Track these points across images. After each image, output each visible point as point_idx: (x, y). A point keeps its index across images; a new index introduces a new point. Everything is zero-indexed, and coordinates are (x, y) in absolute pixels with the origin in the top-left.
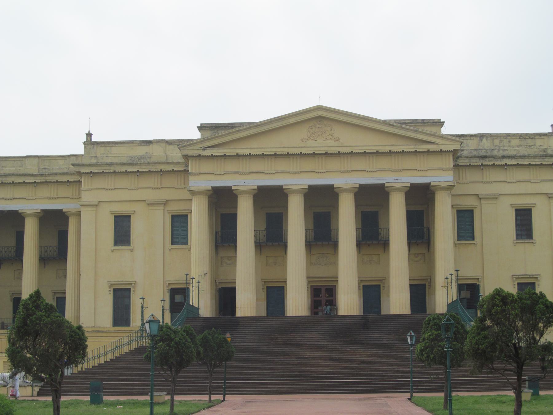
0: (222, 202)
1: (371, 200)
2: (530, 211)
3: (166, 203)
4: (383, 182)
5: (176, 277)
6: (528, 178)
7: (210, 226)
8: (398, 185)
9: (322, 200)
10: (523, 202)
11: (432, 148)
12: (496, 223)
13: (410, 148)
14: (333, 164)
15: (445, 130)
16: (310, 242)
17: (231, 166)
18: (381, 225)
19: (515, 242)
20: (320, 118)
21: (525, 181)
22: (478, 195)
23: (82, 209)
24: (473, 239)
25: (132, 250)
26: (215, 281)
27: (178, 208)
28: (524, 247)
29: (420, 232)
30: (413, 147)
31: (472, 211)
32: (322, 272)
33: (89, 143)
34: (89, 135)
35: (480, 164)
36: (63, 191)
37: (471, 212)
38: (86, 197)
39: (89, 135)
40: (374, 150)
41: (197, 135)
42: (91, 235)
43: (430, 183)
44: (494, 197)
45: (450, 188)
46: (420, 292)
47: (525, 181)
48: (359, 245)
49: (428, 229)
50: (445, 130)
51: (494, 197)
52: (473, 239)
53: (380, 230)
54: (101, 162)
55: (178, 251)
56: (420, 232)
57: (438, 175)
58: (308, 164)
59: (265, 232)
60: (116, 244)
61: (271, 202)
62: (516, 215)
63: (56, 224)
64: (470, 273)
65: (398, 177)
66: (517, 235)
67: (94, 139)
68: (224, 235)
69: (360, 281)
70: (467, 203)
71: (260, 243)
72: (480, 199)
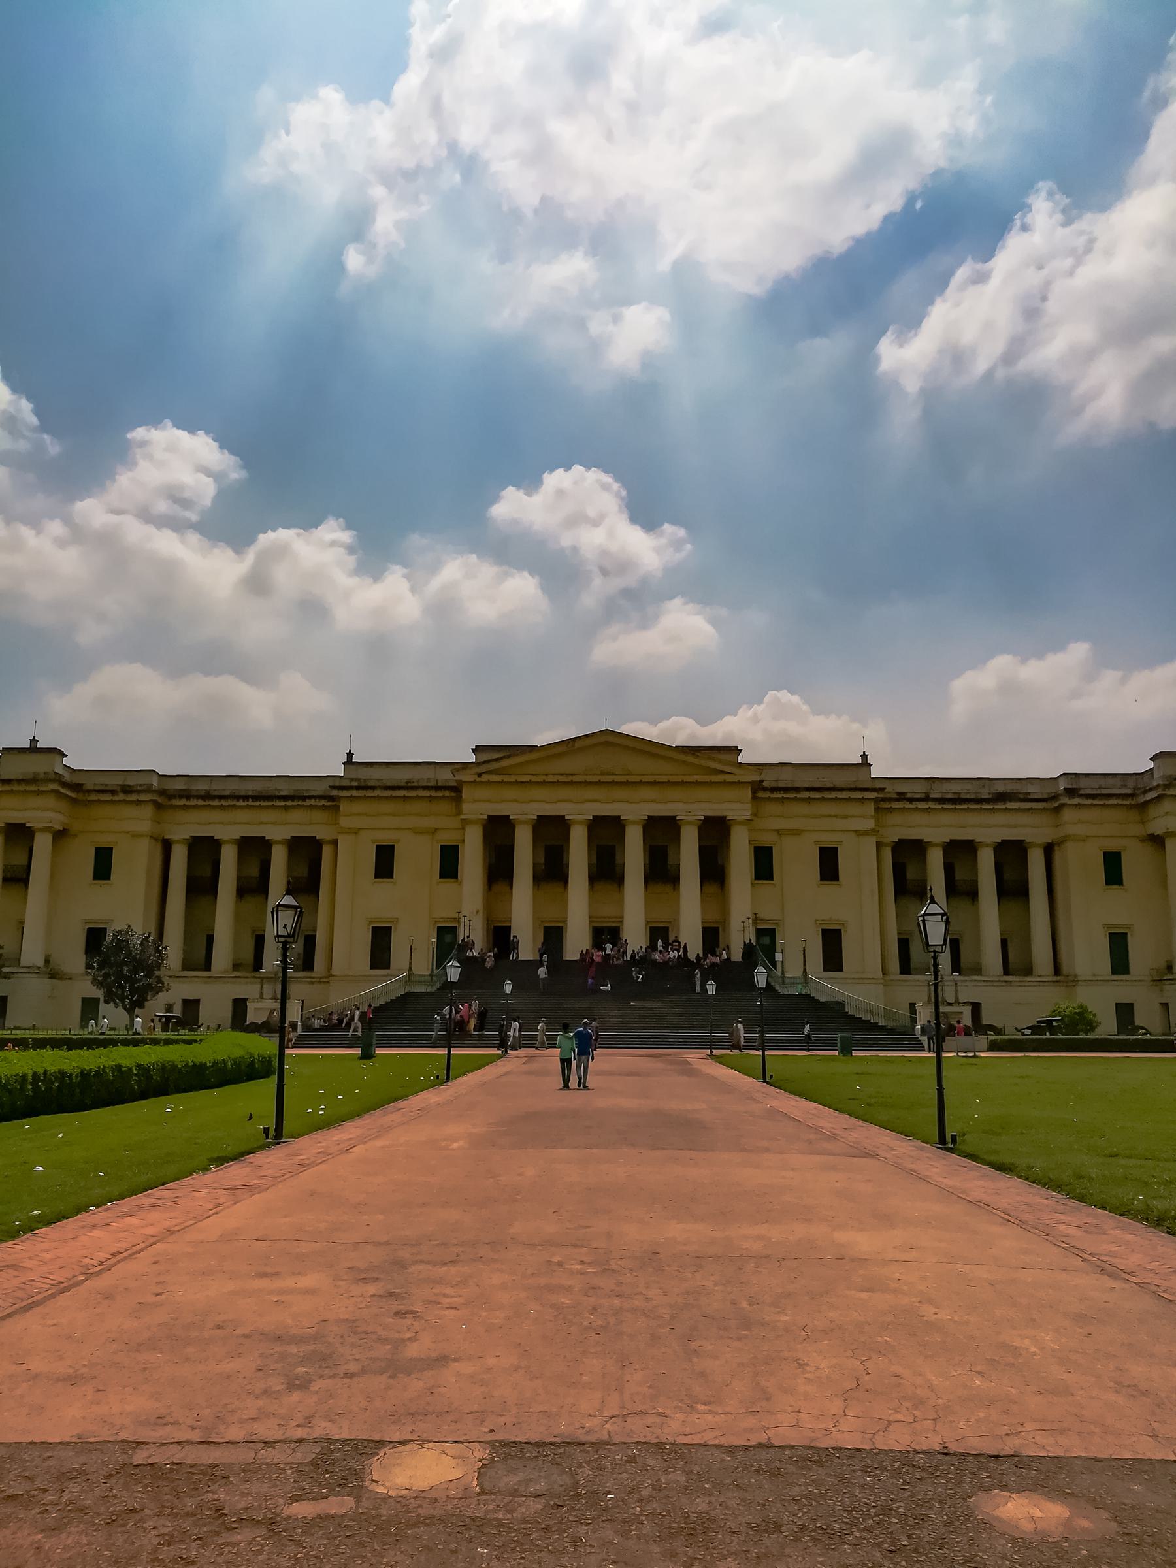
0: (498, 832)
1: (660, 833)
5: (445, 914)
7: (485, 860)
9: (606, 833)
10: (828, 840)
11: (729, 778)
12: (797, 863)
13: (707, 778)
14: (619, 793)
15: (741, 759)
17: (510, 793)
18: (671, 860)
22: (778, 831)
23: (341, 838)
26: (488, 920)
27: (449, 838)
28: (829, 888)
29: (714, 872)
31: (771, 848)
32: (607, 912)
33: (349, 761)
34: (350, 755)
36: (318, 816)
38: (344, 822)
39: (350, 755)
40: (664, 779)
41: (472, 758)
42: (348, 867)
44: (796, 833)
45: (747, 822)
46: (712, 936)
48: (646, 882)
50: (741, 759)
51: (796, 833)
54: (365, 784)
55: (448, 885)
56: (714, 872)
57: (734, 806)
58: (591, 793)
61: (553, 833)
63: (308, 853)
64: (769, 913)
65: (690, 809)
68: (499, 871)
69: (648, 922)
70: (766, 840)
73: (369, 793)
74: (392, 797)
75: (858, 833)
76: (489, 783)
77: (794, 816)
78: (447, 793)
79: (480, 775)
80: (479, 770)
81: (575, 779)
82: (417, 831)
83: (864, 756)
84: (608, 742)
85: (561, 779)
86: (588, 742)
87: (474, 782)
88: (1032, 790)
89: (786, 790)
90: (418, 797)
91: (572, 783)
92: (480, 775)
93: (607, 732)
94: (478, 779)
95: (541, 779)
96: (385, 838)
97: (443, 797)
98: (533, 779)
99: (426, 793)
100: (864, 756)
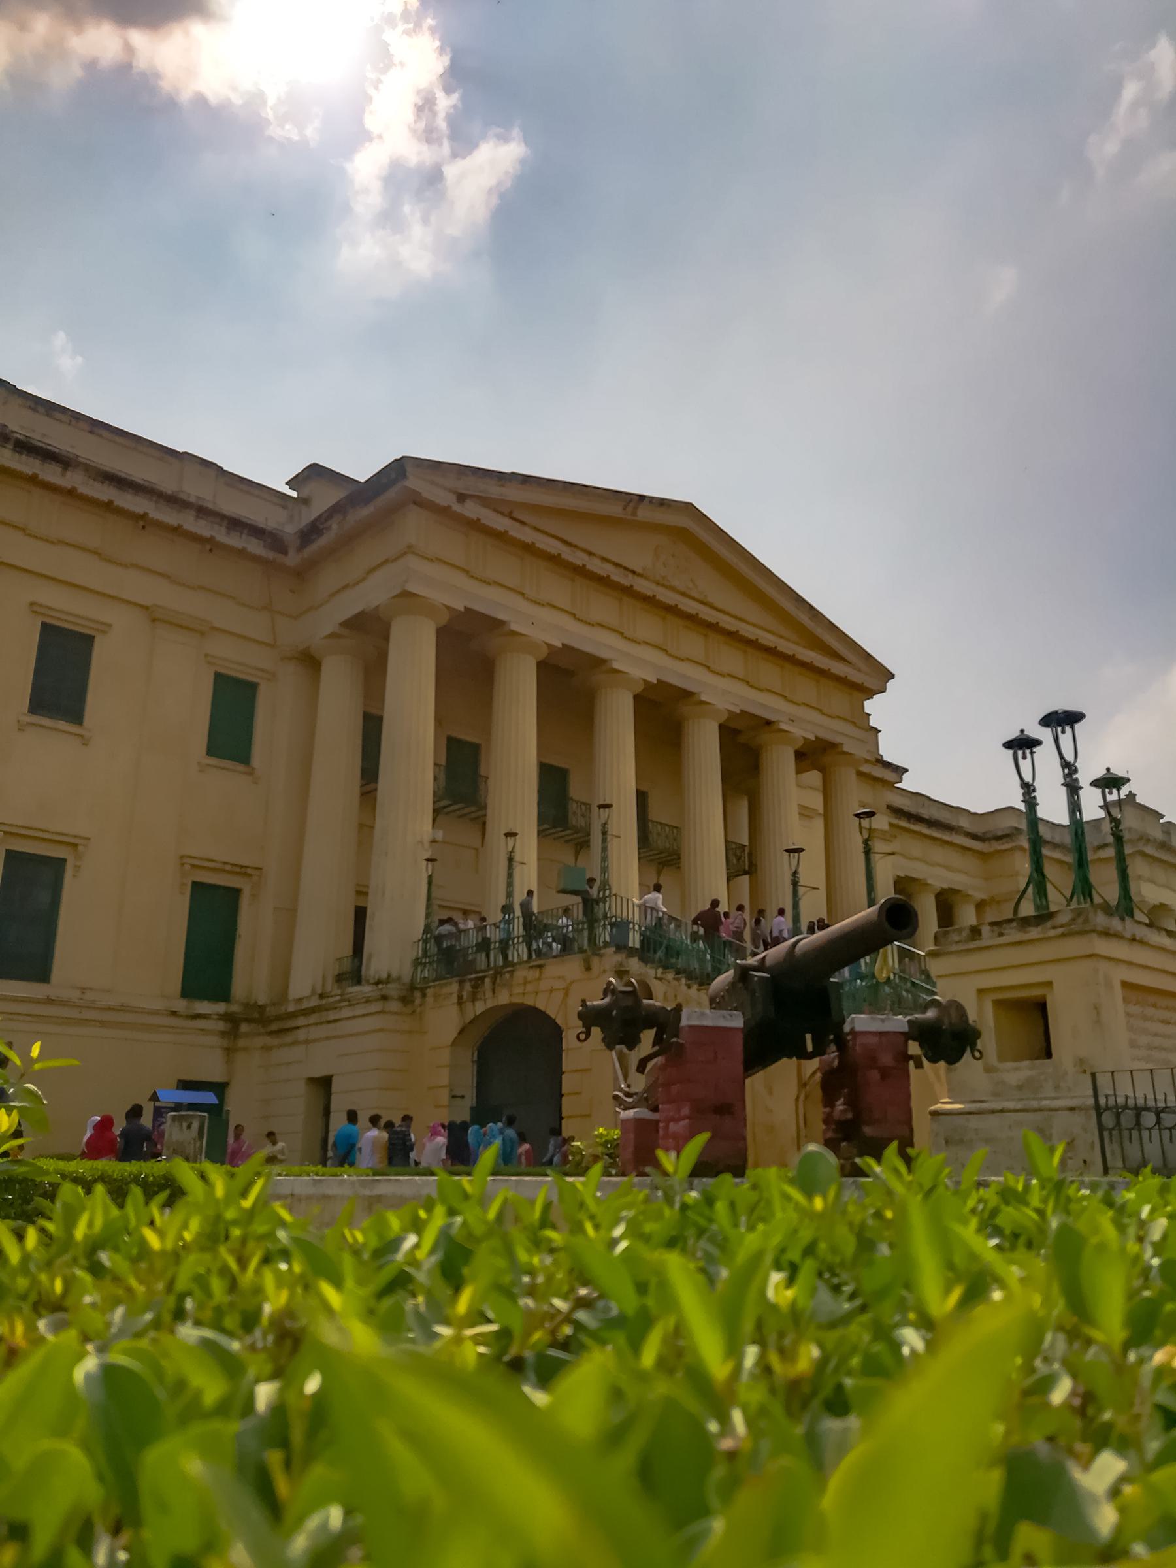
3: (200, 630)
20: (681, 535)
73: (51, 473)
76: (475, 526)
78: (255, 547)
79: (462, 498)
82: (155, 617)
85: (617, 576)
86: (661, 517)
87: (443, 512)
88: (964, 823)
91: (629, 591)
92: (462, 498)
93: (688, 509)
94: (457, 507)
95: (579, 559)
97: (242, 553)
98: (567, 554)
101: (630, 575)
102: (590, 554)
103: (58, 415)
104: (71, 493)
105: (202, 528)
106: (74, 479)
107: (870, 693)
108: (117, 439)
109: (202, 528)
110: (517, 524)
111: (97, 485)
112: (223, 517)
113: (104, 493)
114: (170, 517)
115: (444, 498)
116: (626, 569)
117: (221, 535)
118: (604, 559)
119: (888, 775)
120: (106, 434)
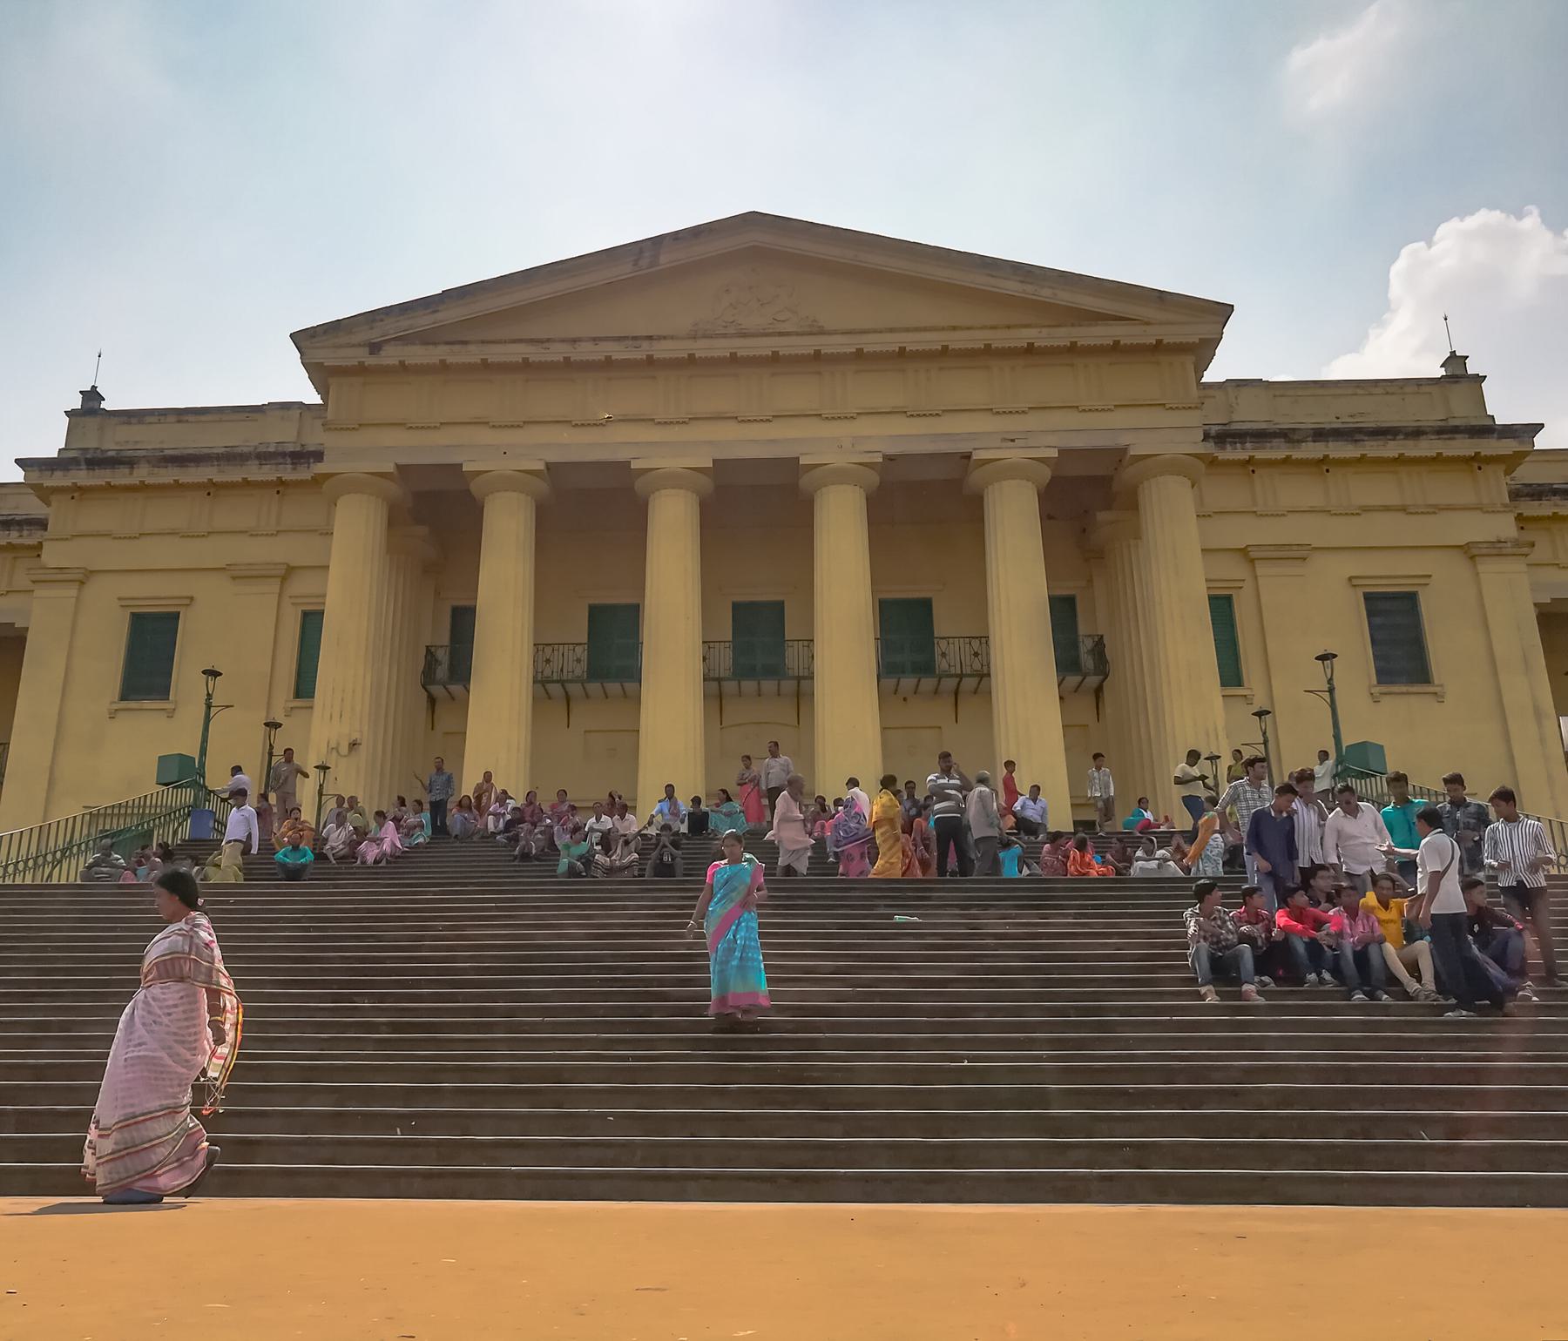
2: (1411, 598)
4: (963, 447)
6: (1393, 500)
8: (1014, 455)
10: (1390, 572)
14: (796, 393)
16: (719, 680)
19: (1376, 690)
21: (1387, 509)
22: (1244, 551)
24: (1240, 684)
25: (171, 714)
30: (1062, 331)
34: (92, 396)
35: (1244, 456)
37: (1229, 598)
38: (53, 555)
39: (92, 396)
40: (931, 341)
43: (1124, 450)
44: (1295, 554)
47: (1387, 509)
49: (1099, 644)
51: (1295, 554)
52: (1240, 684)
53: (943, 644)
59: (582, 653)
60: (124, 697)
62: (1370, 614)
66: (1379, 672)
67: (103, 405)
71: (562, 682)
72: (1252, 561)
73: (121, 477)
74: (178, 486)
75: (1471, 552)
76: (403, 368)
77: (1292, 507)
79: (375, 348)
80: (375, 335)
81: (662, 350)
82: (241, 575)
83: (1455, 361)
84: (759, 248)
85: (619, 352)
87: (361, 370)
89: (1261, 436)
90: (246, 483)
95: (556, 353)
96: (153, 592)
99: (267, 473)
100: (1455, 361)
101: (645, 344)
102: (574, 341)
103: (149, 419)
104: (143, 488)
105: (256, 473)
106: (142, 474)
107: (1205, 350)
108: (203, 418)
109: (267, 473)
110: (456, 348)
111: (163, 471)
112: (284, 455)
113: (167, 476)
114: (234, 475)
115: (362, 356)
116: (635, 338)
117: (288, 474)
118: (595, 340)
119: (1507, 447)
120: (191, 418)
